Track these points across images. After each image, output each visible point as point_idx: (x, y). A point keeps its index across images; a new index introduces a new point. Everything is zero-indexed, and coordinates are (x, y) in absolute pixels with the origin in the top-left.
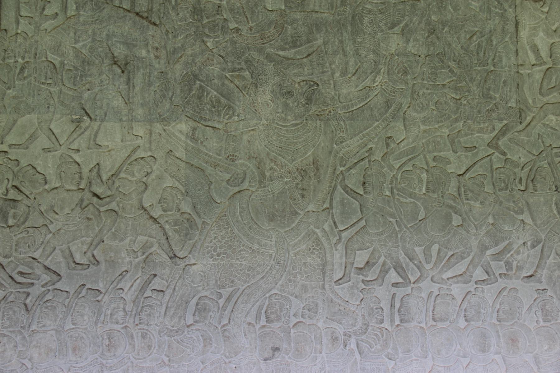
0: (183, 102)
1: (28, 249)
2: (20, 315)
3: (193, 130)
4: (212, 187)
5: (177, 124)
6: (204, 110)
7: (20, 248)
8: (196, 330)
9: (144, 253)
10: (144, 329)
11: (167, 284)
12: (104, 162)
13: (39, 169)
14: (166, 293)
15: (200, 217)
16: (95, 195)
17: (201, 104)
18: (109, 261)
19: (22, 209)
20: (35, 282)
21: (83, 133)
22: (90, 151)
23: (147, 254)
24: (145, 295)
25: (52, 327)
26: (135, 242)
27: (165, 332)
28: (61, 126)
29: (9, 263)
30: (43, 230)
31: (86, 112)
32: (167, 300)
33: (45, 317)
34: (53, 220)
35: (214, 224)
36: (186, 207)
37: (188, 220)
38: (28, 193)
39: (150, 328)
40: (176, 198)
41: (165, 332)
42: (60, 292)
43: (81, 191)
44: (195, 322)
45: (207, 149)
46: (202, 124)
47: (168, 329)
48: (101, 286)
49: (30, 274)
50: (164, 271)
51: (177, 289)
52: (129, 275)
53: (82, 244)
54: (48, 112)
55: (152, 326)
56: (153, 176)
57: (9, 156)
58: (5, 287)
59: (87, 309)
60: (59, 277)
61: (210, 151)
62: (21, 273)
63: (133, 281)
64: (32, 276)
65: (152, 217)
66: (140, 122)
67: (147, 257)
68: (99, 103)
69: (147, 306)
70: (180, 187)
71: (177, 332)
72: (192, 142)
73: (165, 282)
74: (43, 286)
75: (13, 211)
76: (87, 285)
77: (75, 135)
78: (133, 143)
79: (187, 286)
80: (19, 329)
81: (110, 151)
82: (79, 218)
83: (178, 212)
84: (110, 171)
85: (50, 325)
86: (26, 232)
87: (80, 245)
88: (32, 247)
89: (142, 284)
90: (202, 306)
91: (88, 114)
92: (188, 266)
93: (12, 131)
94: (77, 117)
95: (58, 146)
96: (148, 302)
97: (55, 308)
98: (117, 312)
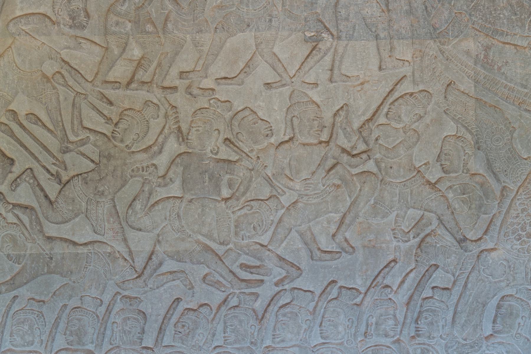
0: (468, 7)
1: (254, 232)
2: (249, 326)
3: (485, 50)
4: (515, 135)
5: (460, 41)
6: (500, 18)
7: (243, 230)
8: (500, 343)
9: (418, 235)
10: (424, 344)
11: (453, 279)
12: (354, 100)
13: (260, 114)
14: (453, 292)
15: (498, 180)
16: (344, 150)
17: (495, 10)
18: (368, 247)
19: (242, 174)
20: (265, 278)
21: (322, 57)
22: (334, 84)
23: (422, 235)
24: (424, 295)
25: (293, 343)
26: (404, 219)
27: (455, 348)
28: (288, 48)
29: (226, 251)
30: (272, 203)
31: (325, 27)
32: (455, 301)
33: (284, 329)
34: (286, 190)
35: (521, 190)
36: (477, 166)
37: (482, 185)
38: (246, 150)
39: (432, 342)
40: (462, 153)
41: (455, 348)
42: (302, 292)
43: (323, 145)
44: (495, 332)
45: (506, 78)
46: (498, 40)
47: (459, 343)
48: (359, 283)
49: (259, 267)
50: (449, 260)
51: (469, 285)
52: (398, 266)
53: (329, 222)
54: (270, 28)
55: (435, 340)
56: (427, 120)
57: (217, 96)
58: (224, 286)
59: (342, 317)
60: (299, 272)
61: (511, 81)
62: (244, 267)
63: (404, 274)
64: (262, 271)
65: (429, 183)
66: (406, 39)
67: (423, 240)
68: (343, 12)
69: (427, 311)
70: (469, 136)
71: (472, 347)
72: (485, 69)
73: (450, 275)
74: (276, 284)
75: (228, 176)
76: (339, 281)
77: (311, 61)
78: (397, 71)
79: (484, 281)
80: (249, 345)
81: (362, 84)
82: (324, 186)
83: (466, 173)
84: (363, 114)
85: (291, 340)
86: (249, 208)
87: (325, 224)
88: (258, 228)
89: (418, 279)
90: (506, 309)
91: (328, 30)
92: (485, 253)
93: (219, 57)
94: (312, 34)
95: (288, 79)
96: (428, 305)
97: (297, 315)
98: (385, 320)
